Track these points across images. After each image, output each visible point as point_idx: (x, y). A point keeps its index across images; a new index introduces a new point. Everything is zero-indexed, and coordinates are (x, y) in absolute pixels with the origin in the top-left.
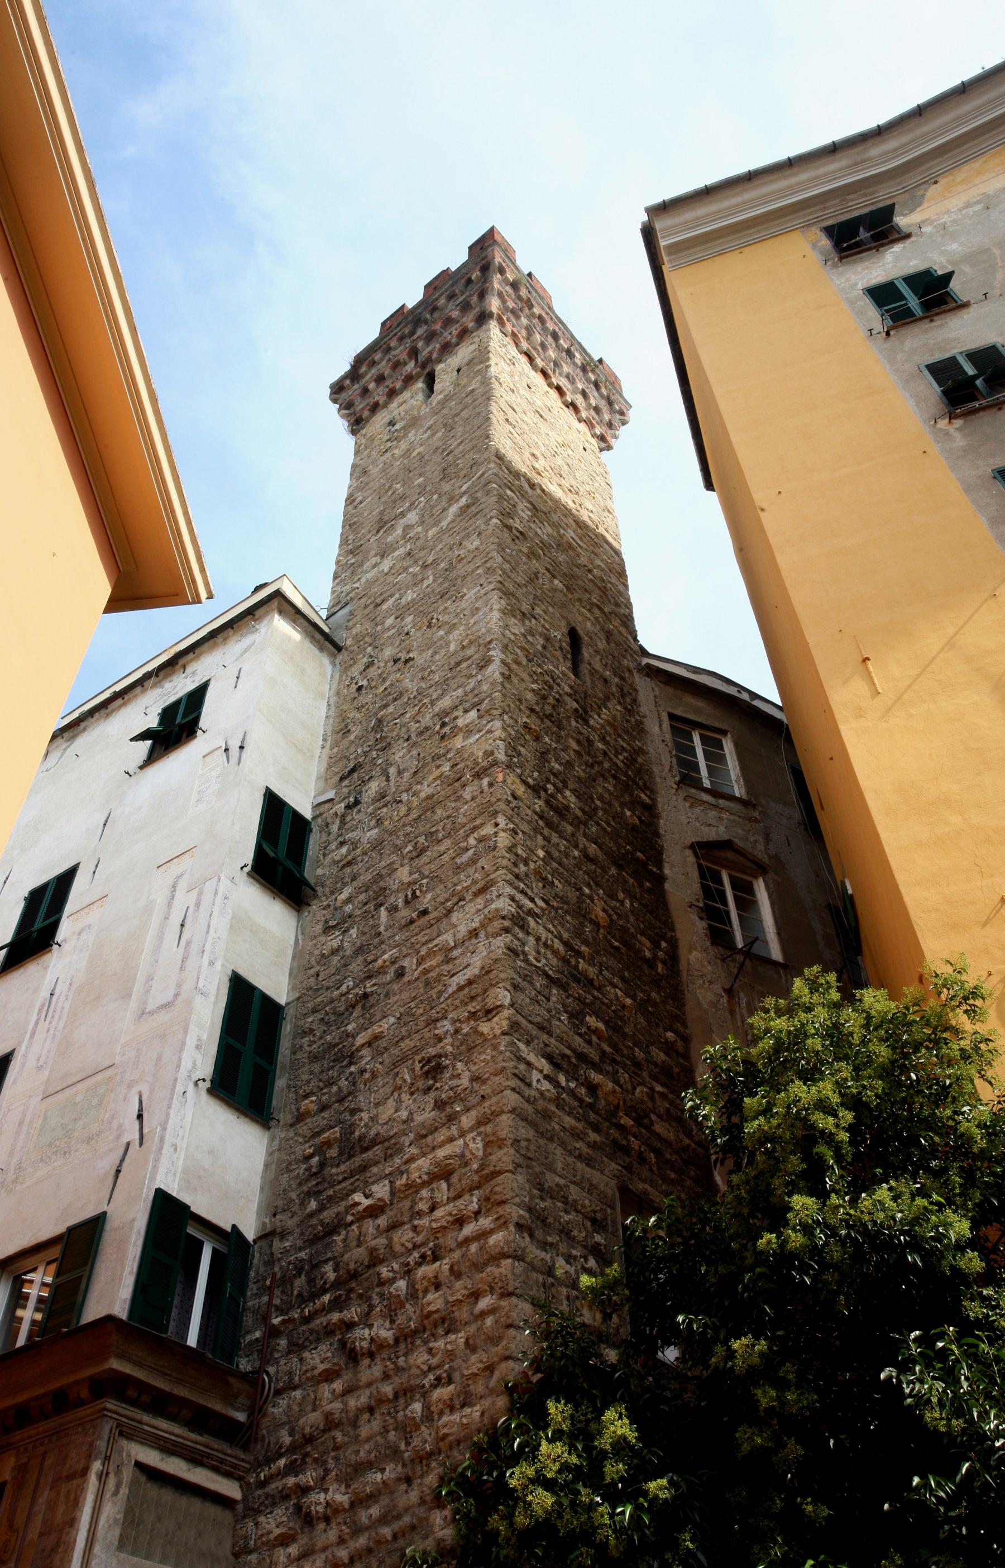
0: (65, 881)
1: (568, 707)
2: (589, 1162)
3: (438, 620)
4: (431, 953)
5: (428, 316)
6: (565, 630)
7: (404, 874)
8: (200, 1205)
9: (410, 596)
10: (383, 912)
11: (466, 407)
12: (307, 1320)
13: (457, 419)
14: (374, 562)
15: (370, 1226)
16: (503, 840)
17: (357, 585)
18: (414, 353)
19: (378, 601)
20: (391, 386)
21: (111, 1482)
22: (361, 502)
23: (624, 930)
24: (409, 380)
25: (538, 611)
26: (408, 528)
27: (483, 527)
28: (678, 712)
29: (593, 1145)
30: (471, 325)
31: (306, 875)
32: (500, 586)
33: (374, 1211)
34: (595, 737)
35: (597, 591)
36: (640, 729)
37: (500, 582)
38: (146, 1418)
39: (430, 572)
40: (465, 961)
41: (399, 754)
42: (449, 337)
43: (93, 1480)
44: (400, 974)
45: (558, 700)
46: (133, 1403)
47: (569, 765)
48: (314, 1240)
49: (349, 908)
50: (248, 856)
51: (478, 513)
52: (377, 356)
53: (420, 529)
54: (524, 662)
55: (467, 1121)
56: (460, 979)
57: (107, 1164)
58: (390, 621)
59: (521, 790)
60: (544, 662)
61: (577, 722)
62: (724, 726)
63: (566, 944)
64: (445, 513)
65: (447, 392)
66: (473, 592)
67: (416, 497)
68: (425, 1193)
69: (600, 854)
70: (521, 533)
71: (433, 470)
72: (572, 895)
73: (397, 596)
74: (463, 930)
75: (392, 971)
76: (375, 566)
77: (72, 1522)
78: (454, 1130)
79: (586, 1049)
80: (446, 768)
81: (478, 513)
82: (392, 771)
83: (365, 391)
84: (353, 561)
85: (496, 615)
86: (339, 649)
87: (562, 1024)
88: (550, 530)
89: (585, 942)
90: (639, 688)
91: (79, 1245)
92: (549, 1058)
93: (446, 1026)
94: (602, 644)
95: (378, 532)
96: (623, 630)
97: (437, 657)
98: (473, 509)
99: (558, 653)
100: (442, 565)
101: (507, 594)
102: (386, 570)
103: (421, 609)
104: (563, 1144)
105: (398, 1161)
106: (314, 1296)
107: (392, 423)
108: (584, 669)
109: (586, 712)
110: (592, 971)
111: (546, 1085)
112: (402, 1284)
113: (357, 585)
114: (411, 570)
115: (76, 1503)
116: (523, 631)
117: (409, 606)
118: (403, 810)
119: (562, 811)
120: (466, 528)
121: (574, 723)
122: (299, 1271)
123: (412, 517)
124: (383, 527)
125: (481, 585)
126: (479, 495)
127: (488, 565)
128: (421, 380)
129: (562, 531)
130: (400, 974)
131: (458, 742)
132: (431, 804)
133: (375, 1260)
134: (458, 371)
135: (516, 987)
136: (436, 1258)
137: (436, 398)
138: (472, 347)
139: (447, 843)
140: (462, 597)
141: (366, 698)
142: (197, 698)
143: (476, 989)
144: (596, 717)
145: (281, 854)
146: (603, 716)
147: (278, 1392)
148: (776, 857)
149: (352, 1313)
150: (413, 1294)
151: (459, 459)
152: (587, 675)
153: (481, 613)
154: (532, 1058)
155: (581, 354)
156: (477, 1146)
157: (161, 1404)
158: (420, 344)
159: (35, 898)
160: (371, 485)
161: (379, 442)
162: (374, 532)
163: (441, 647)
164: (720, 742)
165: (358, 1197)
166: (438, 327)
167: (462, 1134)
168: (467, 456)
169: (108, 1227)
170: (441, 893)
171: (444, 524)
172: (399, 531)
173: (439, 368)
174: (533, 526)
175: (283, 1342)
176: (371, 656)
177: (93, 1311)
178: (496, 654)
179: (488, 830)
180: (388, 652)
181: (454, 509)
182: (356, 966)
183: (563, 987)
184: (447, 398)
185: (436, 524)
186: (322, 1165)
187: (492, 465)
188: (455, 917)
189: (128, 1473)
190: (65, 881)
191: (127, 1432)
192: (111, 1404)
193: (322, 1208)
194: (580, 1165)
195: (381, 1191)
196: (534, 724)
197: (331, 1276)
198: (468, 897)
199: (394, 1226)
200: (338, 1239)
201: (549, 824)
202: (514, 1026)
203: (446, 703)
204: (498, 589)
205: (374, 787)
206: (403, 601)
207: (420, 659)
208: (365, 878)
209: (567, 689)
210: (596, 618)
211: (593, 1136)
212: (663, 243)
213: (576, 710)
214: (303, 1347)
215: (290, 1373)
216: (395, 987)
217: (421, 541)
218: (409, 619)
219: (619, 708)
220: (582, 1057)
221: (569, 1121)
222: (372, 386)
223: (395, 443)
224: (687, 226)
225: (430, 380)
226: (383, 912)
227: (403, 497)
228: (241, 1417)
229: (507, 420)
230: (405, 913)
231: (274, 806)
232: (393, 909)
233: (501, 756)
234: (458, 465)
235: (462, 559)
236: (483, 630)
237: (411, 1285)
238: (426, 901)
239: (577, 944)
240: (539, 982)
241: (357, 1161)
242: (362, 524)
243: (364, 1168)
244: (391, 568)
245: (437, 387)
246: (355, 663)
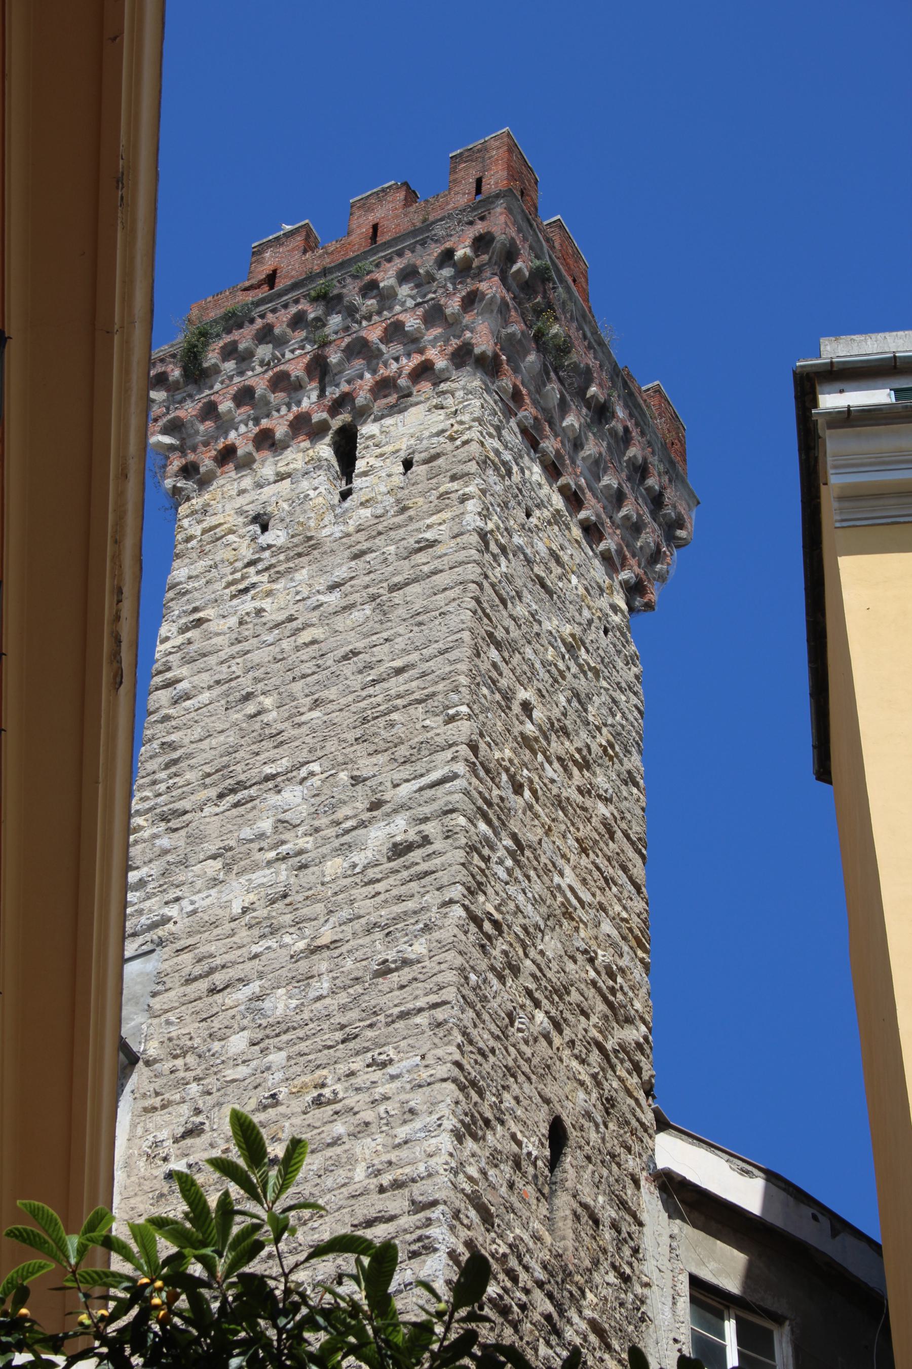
1: (537, 1317)
3: (335, 1093)
5: (358, 300)
6: (544, 1129)
9: (280, 1004)
11: (416, 580)
13: (398, 597)
14: (210, 873)
17: (172, 911)
18: (320, 369)
19: (219, 978)
20: (265, 423)
22: (188, 697)
25: (508, 1101)
26: (283, 824)
27: (433, 913)
28: (706, 1274)
30: (441, 363)
32: (456, 1072)
35: (601, 1007)
37: (458, 1064)
39: (324, 966)
42: (394, 366)
45: (523, 1307)
51: (426, 874)
52: (244, 338)
53: (307, 843)
58: (238, 1043)
60: (509, 1226)
61: (548, 1343)
62: (779, 1306)
64: (361, 831)
65: (380, 511)
66: (406, 1064)
67: (304, 755)
70: (496, 924)
73: (255, 987)
76: (215, 882)
81: (426, 874)
83: (210, 411)
84: (165, 842)
86: (132, 1059)
88: (538, 887)
90: (644, 1217)
95: (221, 796)
96: (633, 1081)
97: (329, 1182)
98: (415, 855)
99: (530, 1189)
100: (349, 964)
101: (469, 1086)
102: (236, 909)
103: (303, 1047)
107: (262, 522)
109: (561, 1312)
113: (172, 911)
114: (287, 939)
116: (483, 1164)
117: (283, 1027)
120: (400, 899)
121: (543, 1350)
124: (233, 791)
125: (423, 1057)
126: (430, 828)
127: (440, 1014)
128: (328, 439)
129: (557, 879)
134: (408, 464)
138: (439, 420)
140: (384, 1065)
144: (576, 1319)
146: (588, 1313)
151: (396, 709)
152: (569, 1223)
153: (418, 1124)
155: (626, 406)
158: (334, 358)
160: (212, 660)
161: (229, 554)
162: (213, 793)
163: (337, 1164)
164: (769, 1335)
166: (374, 334)
168: (411, 710)
171: (360, 858)
172: (266, 825)
173: (368, 429)
174: (512, 889)
176: (198, 1111)
185: (344, 849)
187: (460, 768)
204: (455, 1081)
206: (267, 1004)
209: (540, 1275)
210: (594, 1076)
212: (836, 481)
213: (548, 1317)
217: (308, 877)
218: (277, 1058)
219: (611, 1278)
222: (226, 406)
223: (264, 577)
224: (882, 463)
227: (277, 739)
229: (491, 635)
234: (392, 725)
235: (391, 971)
236: (422, 1168)
242: (189, 756)
244: (245, 910)
245: (357, 483)
246: (164, 1107)
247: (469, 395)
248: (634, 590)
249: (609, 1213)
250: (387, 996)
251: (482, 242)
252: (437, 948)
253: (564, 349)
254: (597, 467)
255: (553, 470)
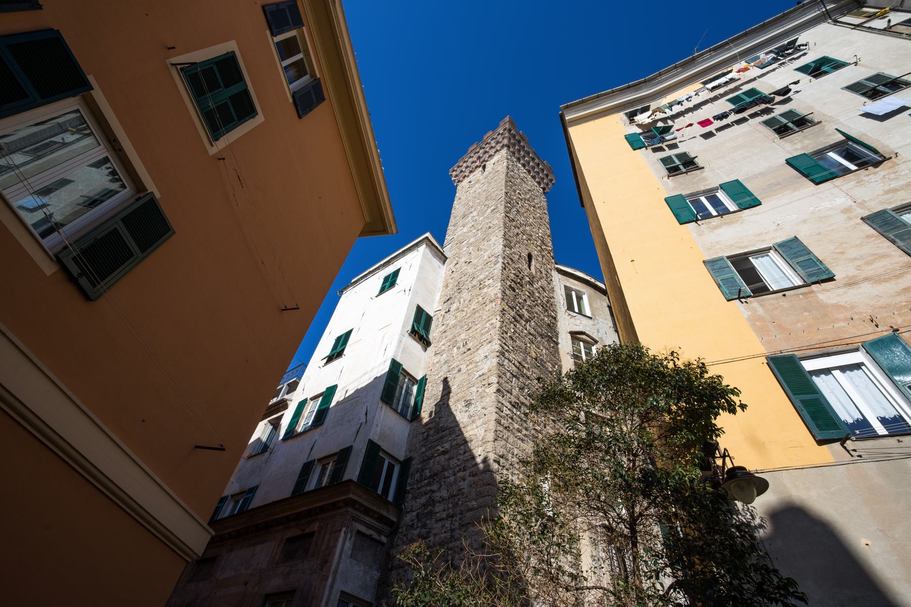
0: (348, 334)
2: (523, 440)
4: (471, 363)
7: (463, 336)
8: (384, 446)
9: (472, 240)
10: (455, 349)
12: (419, 489)
15: (442, 458)
16: (498, 324)
18: (479, 158)
21: (349, 535)
23: (542, 360)
24: (477, 167)
29: (525, 435)
31: (431, 337)
33: (444, 453)
34: (535, 291)
36: (553, 290)
38: (362, 516)
40: (481, 367)
41: (465, 295)
43: (342, 533)
44: (460, 371)
46: (358, 510)
47: (525, 300)
48: (422, 462)
49: (443, 348)
50: (409, 328)
54: (510, 262)
55: (479, 422)
56: (480, 373)
57: (355, 429)
59: (506, 308)
63: (520, 363)
68: (462, 447)
69: (535, 333)
71: (483, 197)
72: (523, 346)
74: (483, 356)
75: (457, 369)
77: (335, 546)
78: (474, 425)
79: (525, 401)
80: (480, 299)
82: (462, 300)
85: (501, 247)
87: (516, 391)
89: (527, 363)
91: (344, 455)
92: (510, 402)
93: (474, 389)
94: (540, 259)
104: (513, 434)
105: (454, 436)
106: (421, 481)
108: (533, 267)
110: (529, 374)
111: (508, 412)
112: (452, 478)
115: (337, 540)
118: (464, 313)
119: (521, 316)
122: (418, 471)
123: (475, 213)
130: (460, 371)
131: (485, 290)
132: (475, 311)
133: (444, 470)
135: (500, 377)
136: (464, 470)
137: (486, 173)
139: (479, 326)
141: (455, 275)
142: (396, 274)
143: (484, 377)
145: (421, 327)
147: (408, 512)
148: (601, 338)
149: (435, 487)
150: (455, 482)
154: (504, 402)
156: (482, 432)
157: (367, 511)
159: (338, 339)
165: (439, 447)
167: (477, 427)
169: (353, 451)
170: (476, 342)
175: (410, 496)
177: (346, 477)
178: (501, 260)
179: (494, 321)
180: (463, 259)
181: (489, 210)
182: (445, 368)
183: (518, 379)
184: (490, 173)
186: (428, 436)
188: (480, 351)
189: (354, 533)
190: (348, 334)
191: (355, 519)
192: (350, 509)
193: (427, 451)
194: (519, 442)
195: (447, 446)
196: (513, 285)
197: (428, 474)
198: (485, 344)
199: (450, 459)
200: (431, 461)
201: (516, 321)
202: (498, 391)
203: (482, 277)
205: (454, 306)
207: (474, 261)
208: (450, 337)
211: (524, 432)
214: (417, 498)
215: (412, 506)
216: (457, 375)
220: (522, 403)
221: (516, 426)
225: (484, 167)
226: (455, 349)
228: (395, 520)
230: (463, 349)
231: (420, 311)
232: (459, 348)
233: (500, 295)
237: (455, 479)
238: (470, 345)
239: (524, 363)
240: (508, 374)
241: (440, 435)
243: (442, 438)
247: (504, 151)
248: (544, 189)
249: (544, 272)
250: (491, 230)
251: (505, 130)
252: (498, 220)
253: (524, 147)
254: (533, 168)
255: (524, 166)
